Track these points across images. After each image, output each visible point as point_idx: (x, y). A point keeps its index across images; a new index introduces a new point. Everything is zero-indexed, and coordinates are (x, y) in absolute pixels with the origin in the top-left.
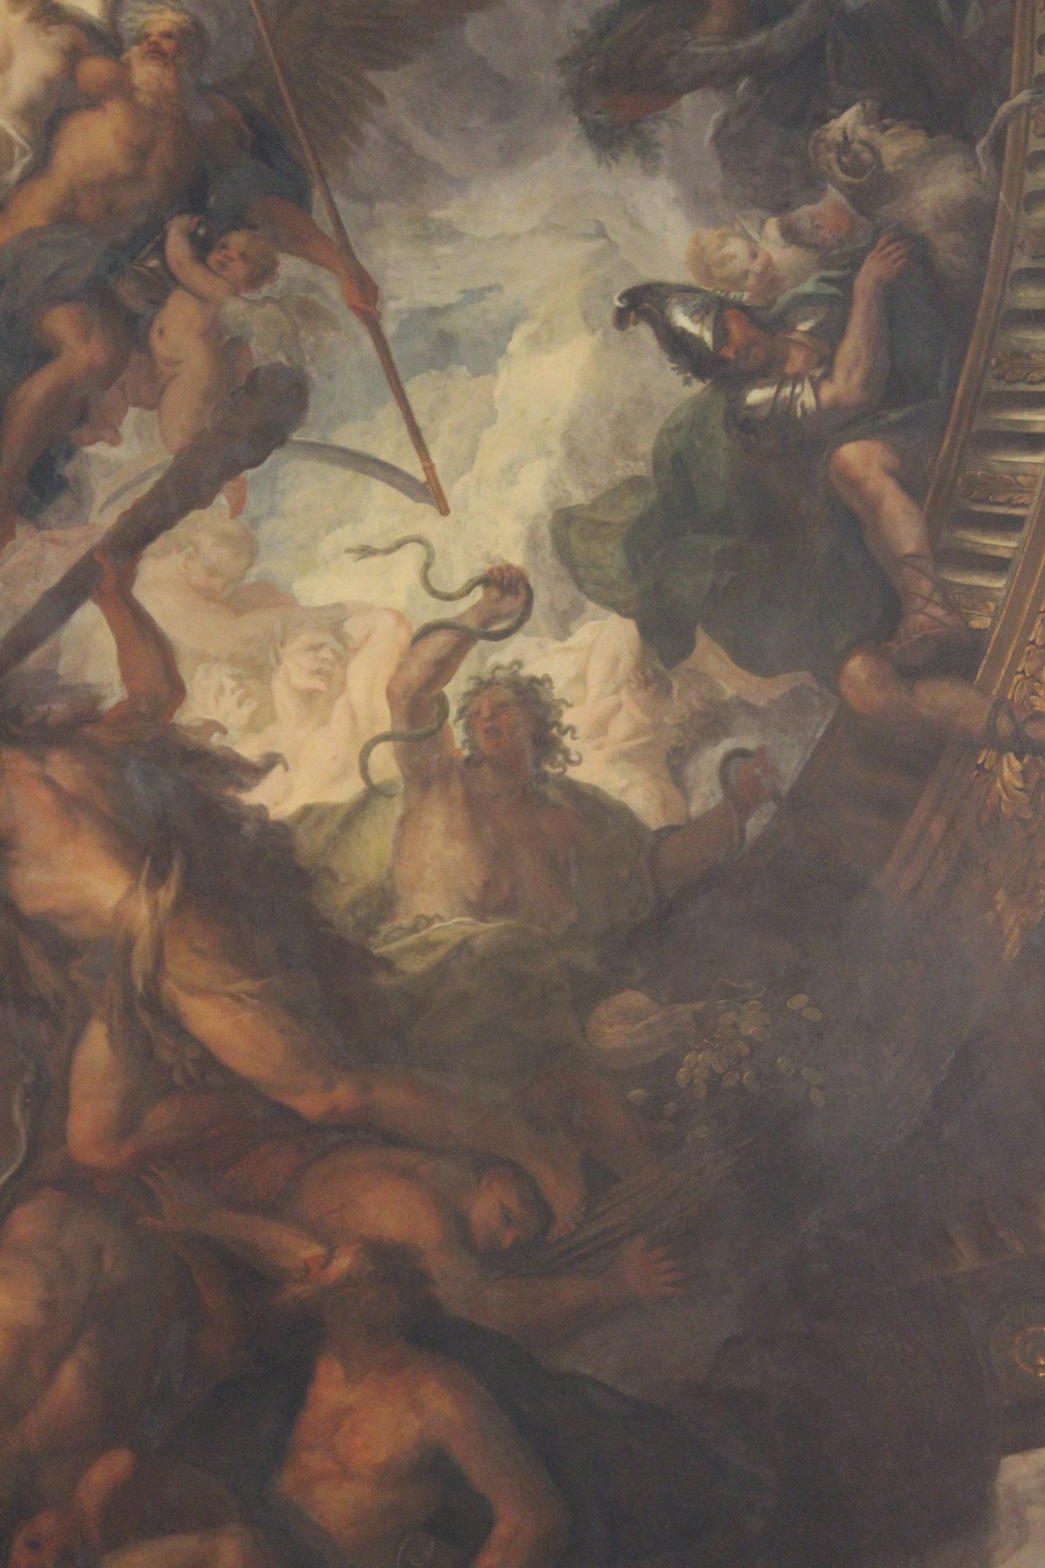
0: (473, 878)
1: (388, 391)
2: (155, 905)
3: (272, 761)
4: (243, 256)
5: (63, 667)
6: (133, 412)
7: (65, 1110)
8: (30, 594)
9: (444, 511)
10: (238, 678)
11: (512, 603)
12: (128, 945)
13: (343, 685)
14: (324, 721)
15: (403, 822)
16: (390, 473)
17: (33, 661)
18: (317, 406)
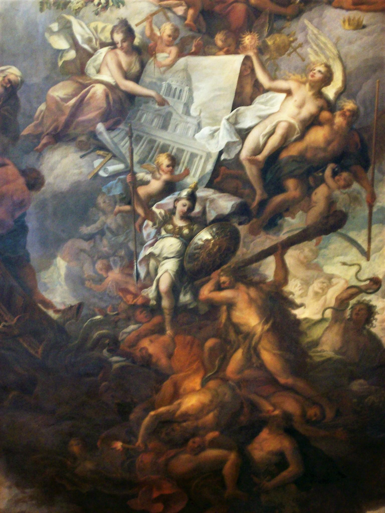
0: (338, 345)
1: (367, 226)
2: (263, 329)
3: (302, 305)
4: (345, 180)
5: (262, 269)
6: (300, 212)
7: (227, 364)
8: (259, 249)
9: (368, 259)
10: (302, 284)
11: (375, 287)
12: (254, 335)
13: (326, 293)
14: (318, 300)
15: (327, 328)
16: (359, 247)
17: (254, 265)
18: (347, 225)
